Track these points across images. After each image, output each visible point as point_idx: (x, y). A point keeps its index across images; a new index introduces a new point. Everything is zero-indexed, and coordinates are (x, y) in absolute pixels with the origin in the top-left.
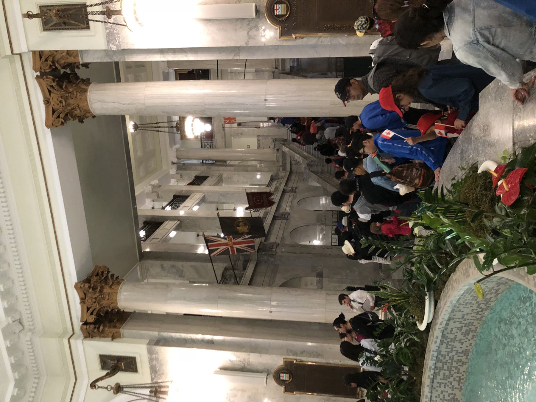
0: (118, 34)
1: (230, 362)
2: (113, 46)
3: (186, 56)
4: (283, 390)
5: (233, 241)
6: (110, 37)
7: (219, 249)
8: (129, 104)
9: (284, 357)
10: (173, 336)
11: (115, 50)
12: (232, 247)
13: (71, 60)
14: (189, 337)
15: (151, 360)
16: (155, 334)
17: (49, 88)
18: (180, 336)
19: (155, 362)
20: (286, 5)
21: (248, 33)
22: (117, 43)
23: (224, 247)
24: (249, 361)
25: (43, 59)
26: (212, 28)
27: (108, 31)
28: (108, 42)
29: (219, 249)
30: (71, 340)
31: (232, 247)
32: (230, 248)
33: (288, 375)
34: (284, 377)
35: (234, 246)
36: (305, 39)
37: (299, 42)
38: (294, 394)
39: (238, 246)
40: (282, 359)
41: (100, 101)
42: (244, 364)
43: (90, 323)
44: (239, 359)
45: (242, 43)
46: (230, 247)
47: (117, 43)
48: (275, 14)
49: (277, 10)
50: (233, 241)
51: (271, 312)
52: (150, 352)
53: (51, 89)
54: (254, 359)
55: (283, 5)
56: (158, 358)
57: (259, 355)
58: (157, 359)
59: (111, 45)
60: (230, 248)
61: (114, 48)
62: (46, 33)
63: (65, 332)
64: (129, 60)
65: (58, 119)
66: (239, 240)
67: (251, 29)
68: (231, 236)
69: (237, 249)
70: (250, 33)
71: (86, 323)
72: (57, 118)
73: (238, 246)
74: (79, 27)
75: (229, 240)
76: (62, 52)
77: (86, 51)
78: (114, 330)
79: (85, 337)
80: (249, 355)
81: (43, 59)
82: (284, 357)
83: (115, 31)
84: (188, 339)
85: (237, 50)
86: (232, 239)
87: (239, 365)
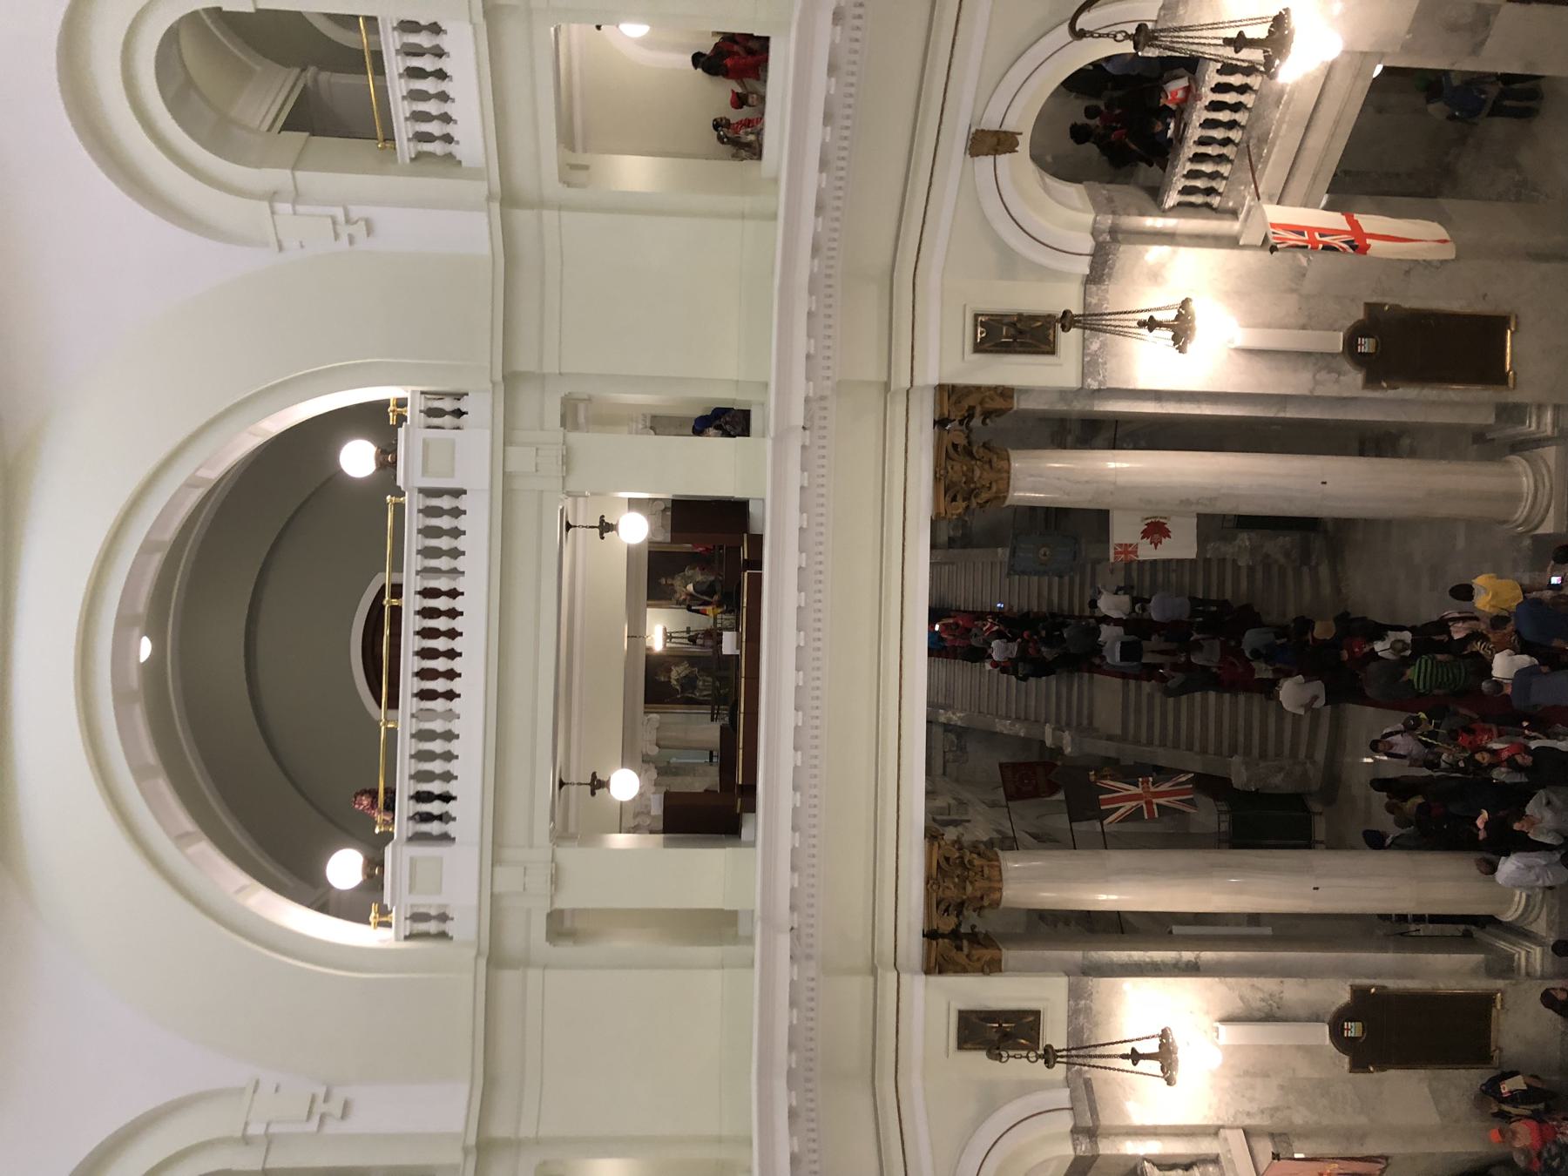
0: (1105, 363)
1: (1241, 1004)
2: (1093, 383)
3: (1199, 407)
4: (1347, 1066)
5: (1152, 789)
6: (1089, 365)
7: (1121, 807)
8: (1087, 482)
9: (1350, 982)
10: (1115, 959)
11: (1095, 388)
12: (1149, 803)
13: (999, 404)
14: (1147, 960)
15: (1073, 1014)
16: (1077, 955)
17: (950, 448)
18: (1130, 956)
19: (1081, 1019)
20: (1374, 340)
21: (1314, 376)
22: (1101, 378)
23: (1134, 803)
24: (1281, 998)
25: (953, 398)
26: (1260, 365)
27: (1087, 359)
28: (1084, 376)
29: (1121, 807)
31: (1149, 803)
32: (1144, 806)
33: (1359, 1025)
34: (1353, 1029)
35: (1155, 801)
36: (1401, 390)
37: (1391, 393)
38: (1370, 1072)
39: (1162, 801)
40: (1348, 989)
41: (1032, 476)
42: (1270, 1005)
43: (943, 936)
44: (1261, 995)
45: (1303, 390)
46: (1146, 803)
47: (1101, 378)
48: (1359, 351)
49: (1361, 345)
50: (1152, 789)
51: (1317, 889)
52: (1075, 994)
53: (951, 451)
54: (1293, 991)
55: (1371, 339)
56: (1091, 1008)
57: (1302, 980)
58: (1088, 1011)
59: (1089, 380)
60: (1144, 806)
61: (1095, 386)
62: (978, 356)
64: (1101, 409)
65: (954, 503)
66: (1165, 787)
67: (1319, 371)
68: (1151, 779)
69: (1157, 804)
70: (1318, 377)
71: (930, 935)
72: (952, 502)
73: (1162, 801)
74: (1038, 349)
75: (1143, 788)
76: (989, 388)
77: (1026, 391)
78: (987, 954)
79: (928, 971)
80: (1282, 982)
81: (953, 398)
82: (1350, 982)
83: (1100, 360)
84: (1147, 964)
85: (1283, 400)
86: (1150, 784)
87: (1259, 1010)
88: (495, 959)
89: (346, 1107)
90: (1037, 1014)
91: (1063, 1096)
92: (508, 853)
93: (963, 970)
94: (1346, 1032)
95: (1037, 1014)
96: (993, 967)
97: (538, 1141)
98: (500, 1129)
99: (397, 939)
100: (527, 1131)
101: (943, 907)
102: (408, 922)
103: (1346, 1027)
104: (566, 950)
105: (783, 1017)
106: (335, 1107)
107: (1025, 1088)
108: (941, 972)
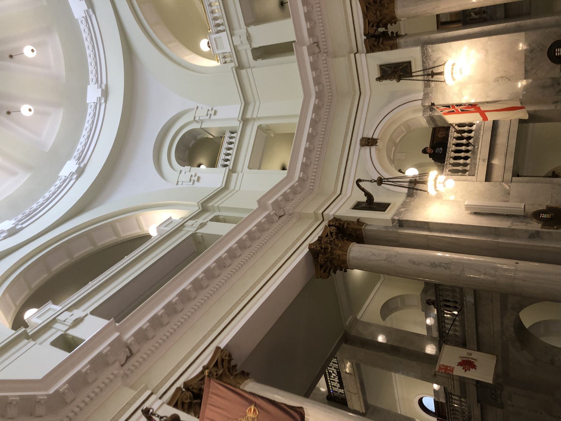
30: (357, 55)
63: (351, 52)
78: (391, 42)
79: (368, 52)
88: (240, 67)
89: (215, 113)
90: (410, 63)
91: (421, 95)
92: (236, 32)
93: (382, 50)
94: (556, 53)
95: (410, 63)
96: (394, 47)
97: (259, 119)
98: (249, 116)
99: (221, 64)
100: (254, 116)
101: (371, 25)
102: (223, 59)
103: (557, 51)
104: (260, 61)
105: (310, 75)
106: (213, 112)
107: (407, 93)
108: (373, 52)
